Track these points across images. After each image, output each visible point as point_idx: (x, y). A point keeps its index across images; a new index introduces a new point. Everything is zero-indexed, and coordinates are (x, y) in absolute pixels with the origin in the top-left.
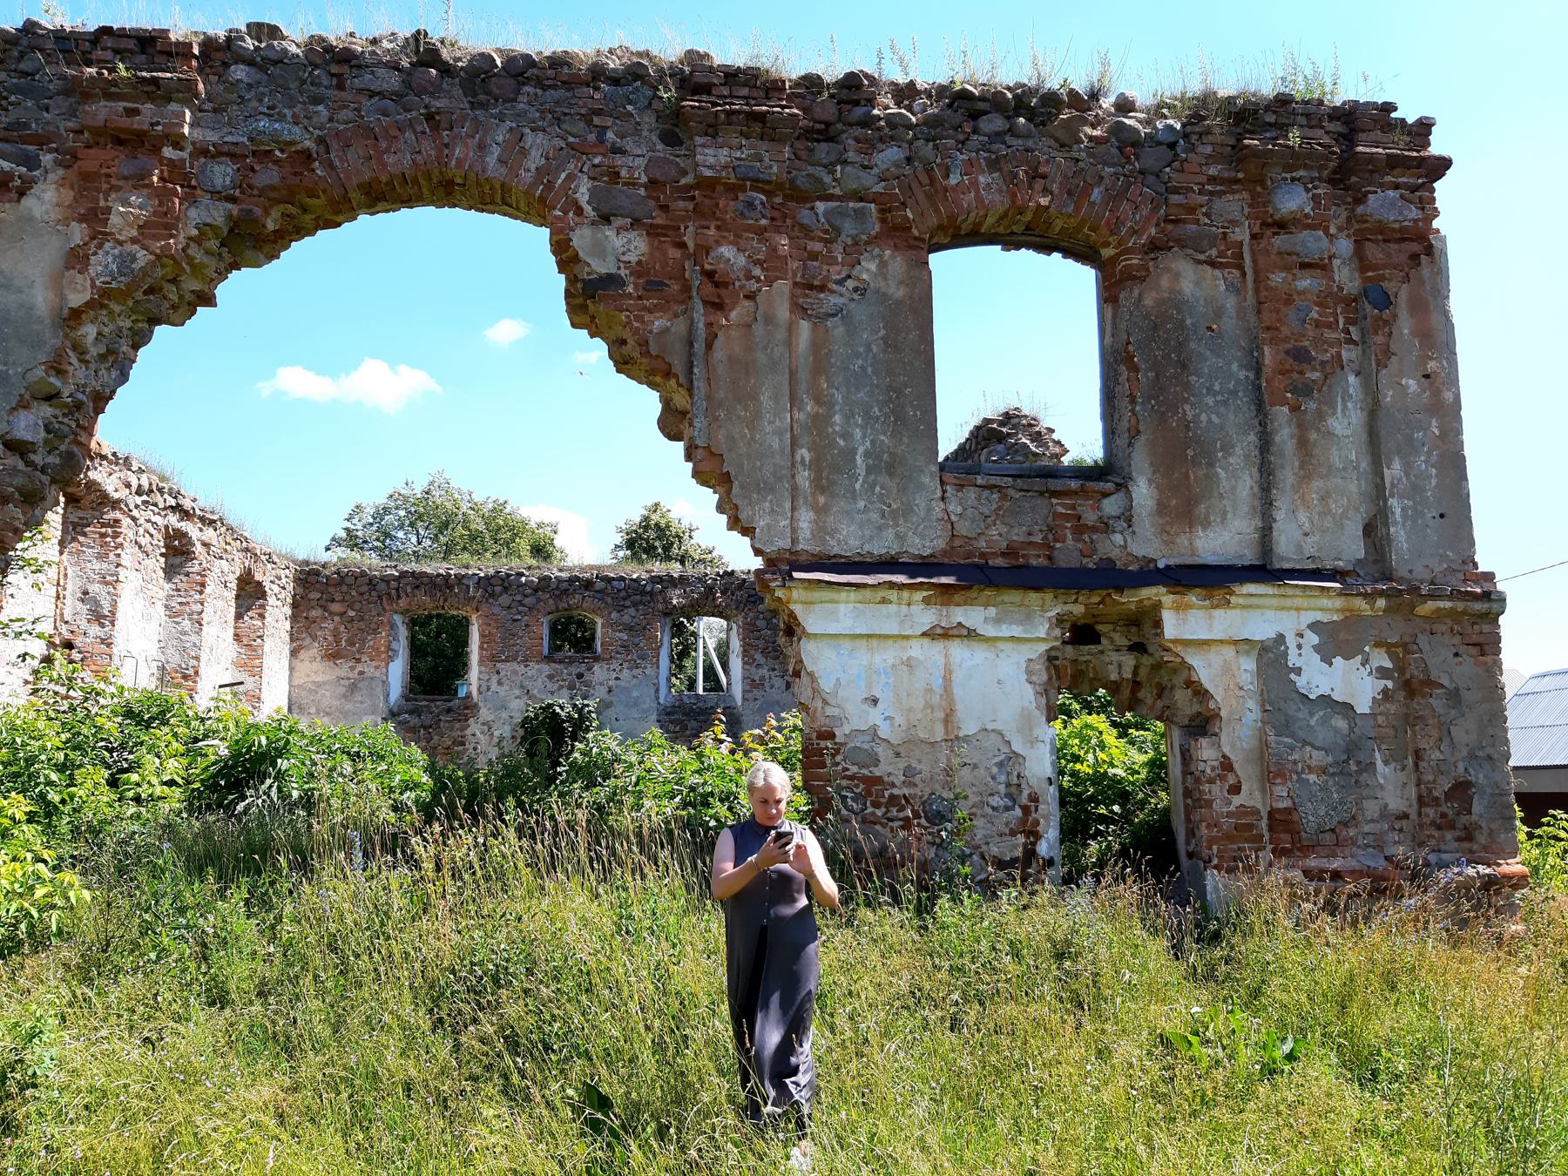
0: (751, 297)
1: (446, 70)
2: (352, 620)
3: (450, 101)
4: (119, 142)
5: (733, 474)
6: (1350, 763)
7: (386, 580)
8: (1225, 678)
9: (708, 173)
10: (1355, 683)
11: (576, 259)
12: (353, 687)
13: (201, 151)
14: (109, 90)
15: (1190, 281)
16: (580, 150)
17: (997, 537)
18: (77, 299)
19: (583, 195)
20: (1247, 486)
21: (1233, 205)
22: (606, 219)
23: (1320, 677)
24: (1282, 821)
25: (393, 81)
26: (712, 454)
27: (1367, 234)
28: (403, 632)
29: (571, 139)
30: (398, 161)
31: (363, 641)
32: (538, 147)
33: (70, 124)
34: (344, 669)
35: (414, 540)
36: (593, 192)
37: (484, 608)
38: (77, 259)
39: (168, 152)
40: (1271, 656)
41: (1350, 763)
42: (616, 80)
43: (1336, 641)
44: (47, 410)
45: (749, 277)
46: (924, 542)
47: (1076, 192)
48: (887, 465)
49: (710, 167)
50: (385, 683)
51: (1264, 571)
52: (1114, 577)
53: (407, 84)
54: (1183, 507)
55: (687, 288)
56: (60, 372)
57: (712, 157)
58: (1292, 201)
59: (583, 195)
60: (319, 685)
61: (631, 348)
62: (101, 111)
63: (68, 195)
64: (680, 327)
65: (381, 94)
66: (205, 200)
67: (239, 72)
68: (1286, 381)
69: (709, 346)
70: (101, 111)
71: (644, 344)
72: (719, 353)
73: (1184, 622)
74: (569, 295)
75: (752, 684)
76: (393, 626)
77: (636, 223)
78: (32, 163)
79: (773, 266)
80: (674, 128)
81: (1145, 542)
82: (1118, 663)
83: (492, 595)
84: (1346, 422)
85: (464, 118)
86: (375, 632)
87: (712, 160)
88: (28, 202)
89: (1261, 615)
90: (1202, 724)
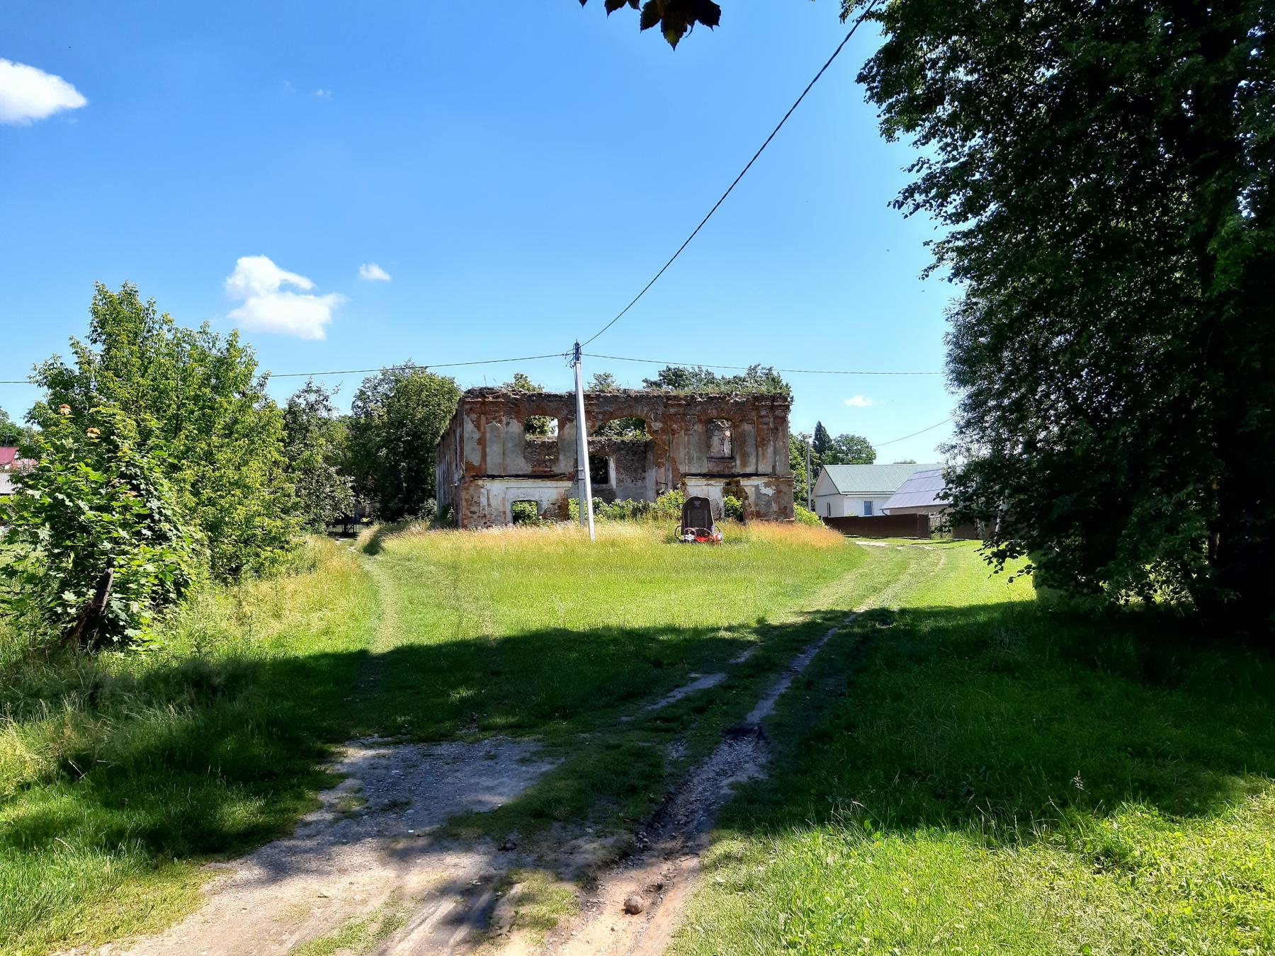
6: (768, 504)
8: (750, 491)
10: (769, 491)
15: (747, 427)
17: (716, 469)
20: (754, 461)
21: (754, 413)
23: (764, 491)
24: (758, 512)
27: (776, 418)
32: (646, 409)
40: (757, 487)
41: (768, 504)
43: (767, 485)
46: (705, 471)
47: (728, 413)
48: (699, 459)
51: (756, 475)
52: (733, 476)
54: (744, 464)
57: (672, 411)
58: (763, 413)
68: (761, 443)
73: (744, 482)
75: (619, 481)
81: (738, 470)
82: (734, 489)
84: (770, 450)
89: (756, 481)
90: (746, 498)
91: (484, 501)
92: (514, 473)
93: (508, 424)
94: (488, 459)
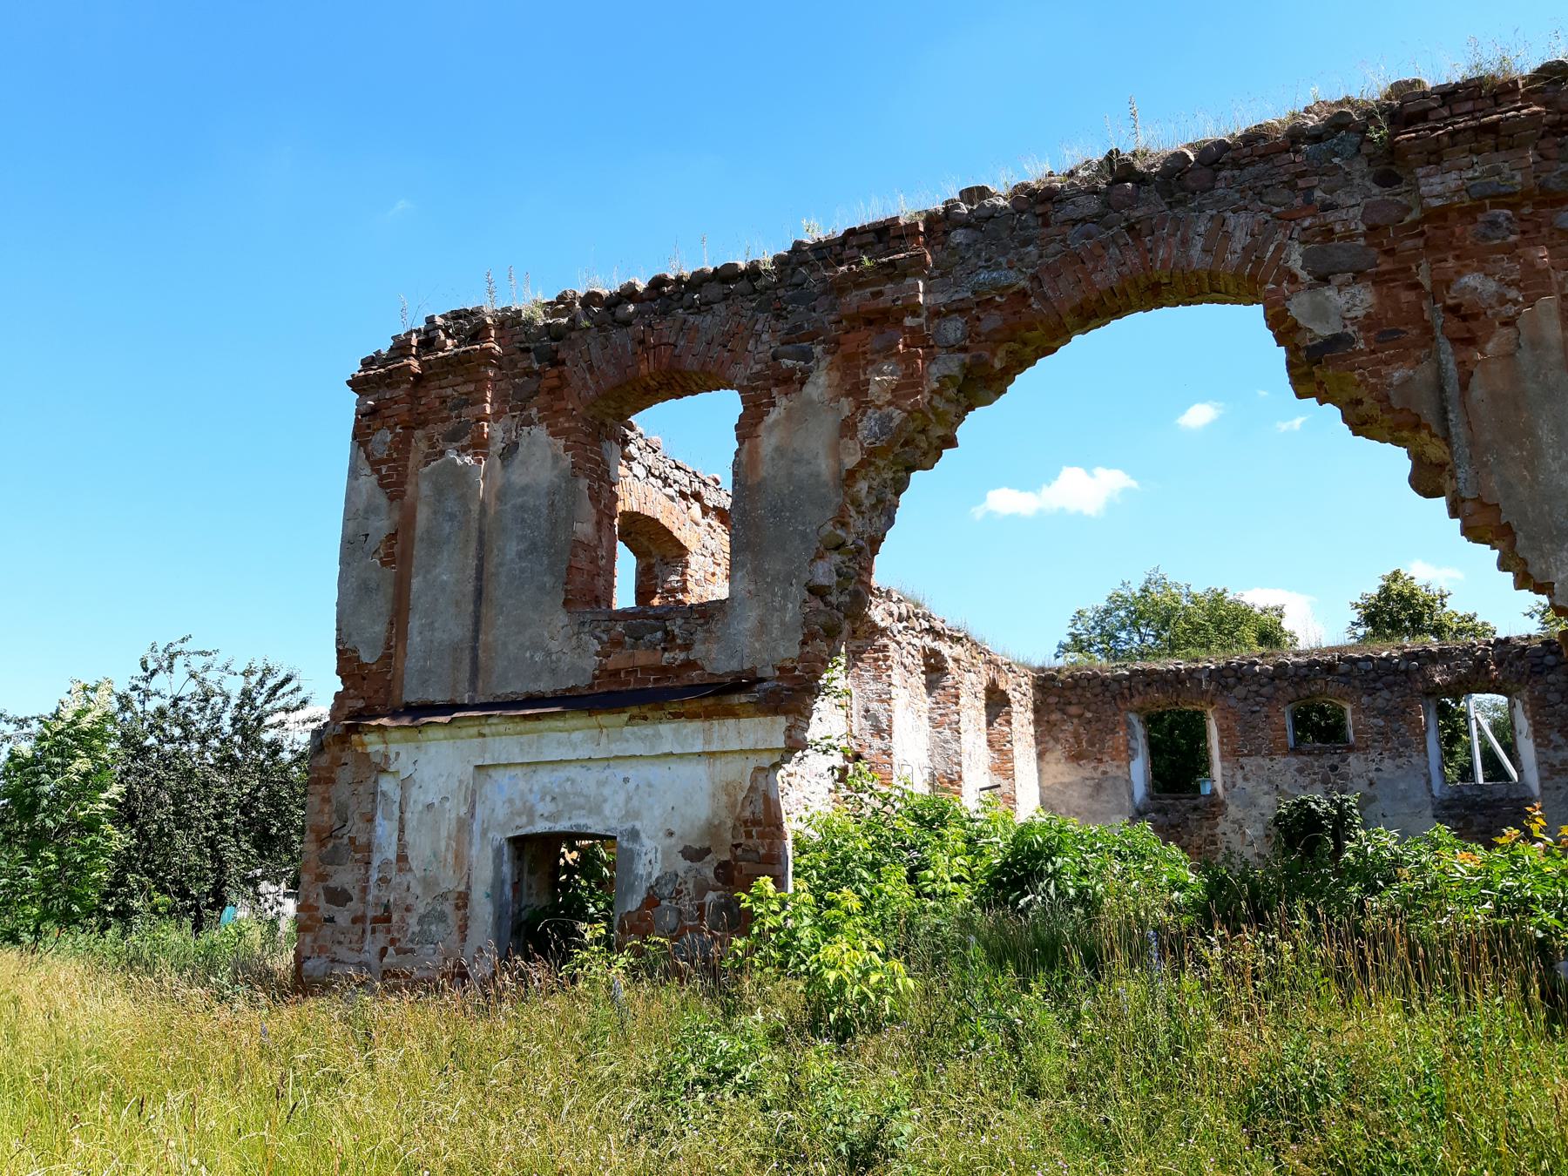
0: (1509, 322)
1: (1141, 179)
2: (1089, 722)
3: (1150, 207)
4: (870, 322)
5: (1514, 524)
7: (1118, 680)
9: (1437, 203)
11: (1296, 327)
12: (1098, 788)
13: (935, 313)
14: (856, 281)
16: (1287, 218)
18: (851, 461)
19: (1295, 261)
22: (1324, 280)
25: (1093, 205)
26: (1485, 505)
28: (1140, 731)
29: (1276, 210)
30: (1106, 277)
31: (1103, 741)
32: (1241, 228)
33: (832, 318)
34: (1087, 770)
35: (1137, 638)
36: (1306, 257)
37: (1219, 702)
38: (848, 428)
39: (909, 321)
42: (1316, 137)
44: (836, 558)
45: (1503, 301)
49: (1437, 196)
50: (1129, 782)
53: (1107, 205)
55: (1428, 330)
56: (844, 525)
57: (1438, 186)
59: (1295, 261)
60: (1066, 786)
61: (1369, 407)
62: (854, 300)
63: (836, 375)
64: (1425, 372)
65: (1083, 220)
66: (942, 355)
67: (958, 237)
69: (1464, 386)
70: (854, 300)
71: (1384, 399)
72: (1478, 391)
74: (1290, 366)
76: (1129, 725)
77: (1359, 275)
78: (807, 356)
79: (1533, 283)
80: (1390, 168)
83: (1226, 687)
85: (1164, 220)
86: (1113, 731)
87: (1439, 188)
88: (809, 389)
91: (385, 830)
92: (517, 687)
93: (510, 451)
94: (415, 623)
